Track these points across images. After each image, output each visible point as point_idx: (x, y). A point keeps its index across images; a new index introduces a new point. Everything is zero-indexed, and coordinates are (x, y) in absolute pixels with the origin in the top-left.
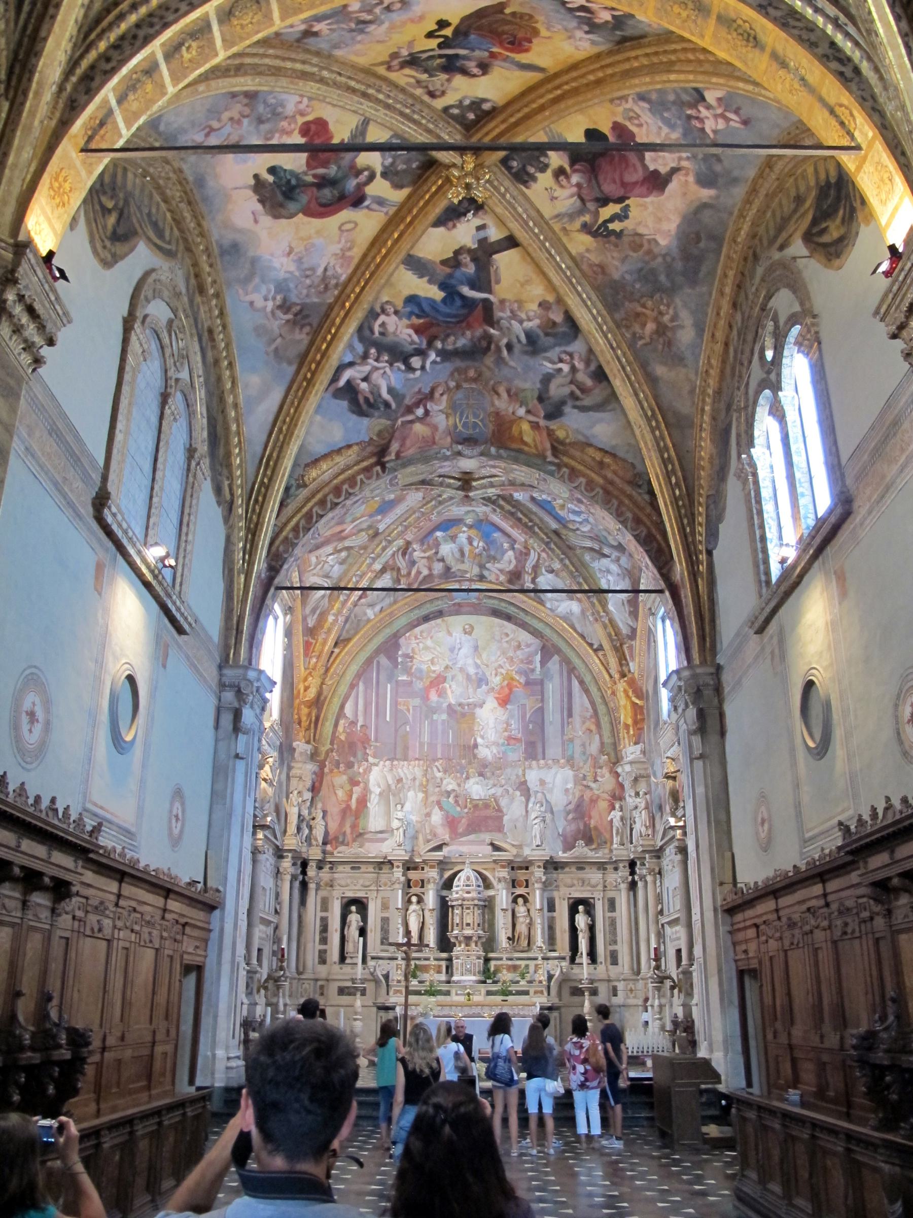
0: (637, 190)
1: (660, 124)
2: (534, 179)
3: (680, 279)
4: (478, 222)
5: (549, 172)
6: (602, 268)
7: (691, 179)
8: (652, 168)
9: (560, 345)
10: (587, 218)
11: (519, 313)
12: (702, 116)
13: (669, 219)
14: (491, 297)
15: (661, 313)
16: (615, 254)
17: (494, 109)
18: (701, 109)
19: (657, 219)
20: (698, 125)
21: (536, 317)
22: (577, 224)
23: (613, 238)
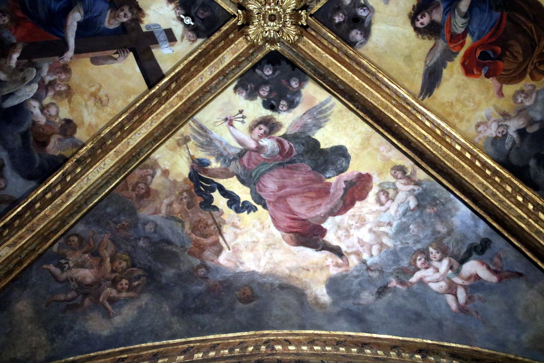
0: (280, 215)
1: (395, 224)
2: (251, 96)
3: (178, 293)
4: (178, 30)
5: (269, 113)
6: (148, 192)
7: (334, 271)
8: (325, 225)
9: (12, 158)
10: (215, 164)
11: (51, 93)
12: (435, 264)
13: (259, 260)
14: (70, 53)
15: (114, 283)
16: (176, 207)
17: (352, 44)
18: (446, 262)
19: (252, 244)
20: (419, 263)
21: (49, 118)
22: (200, 154)
23: (199, 200)
